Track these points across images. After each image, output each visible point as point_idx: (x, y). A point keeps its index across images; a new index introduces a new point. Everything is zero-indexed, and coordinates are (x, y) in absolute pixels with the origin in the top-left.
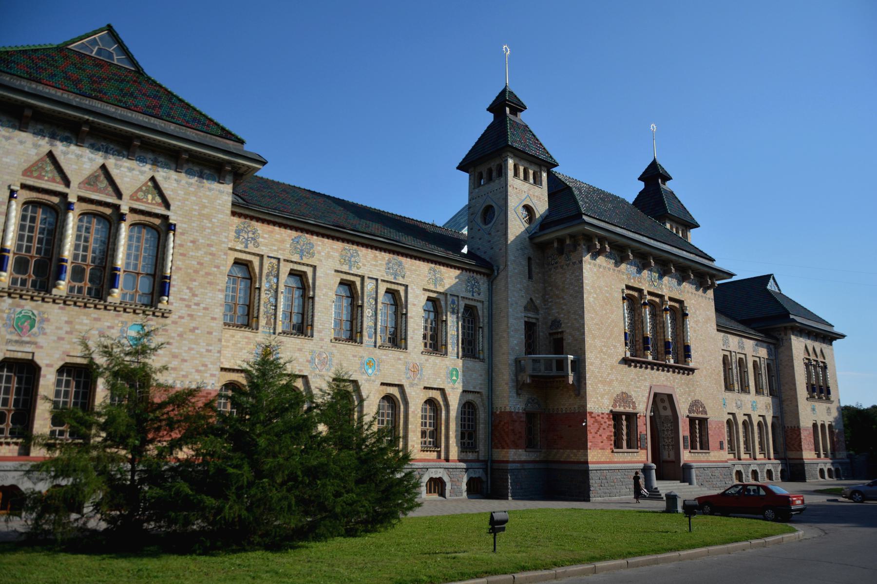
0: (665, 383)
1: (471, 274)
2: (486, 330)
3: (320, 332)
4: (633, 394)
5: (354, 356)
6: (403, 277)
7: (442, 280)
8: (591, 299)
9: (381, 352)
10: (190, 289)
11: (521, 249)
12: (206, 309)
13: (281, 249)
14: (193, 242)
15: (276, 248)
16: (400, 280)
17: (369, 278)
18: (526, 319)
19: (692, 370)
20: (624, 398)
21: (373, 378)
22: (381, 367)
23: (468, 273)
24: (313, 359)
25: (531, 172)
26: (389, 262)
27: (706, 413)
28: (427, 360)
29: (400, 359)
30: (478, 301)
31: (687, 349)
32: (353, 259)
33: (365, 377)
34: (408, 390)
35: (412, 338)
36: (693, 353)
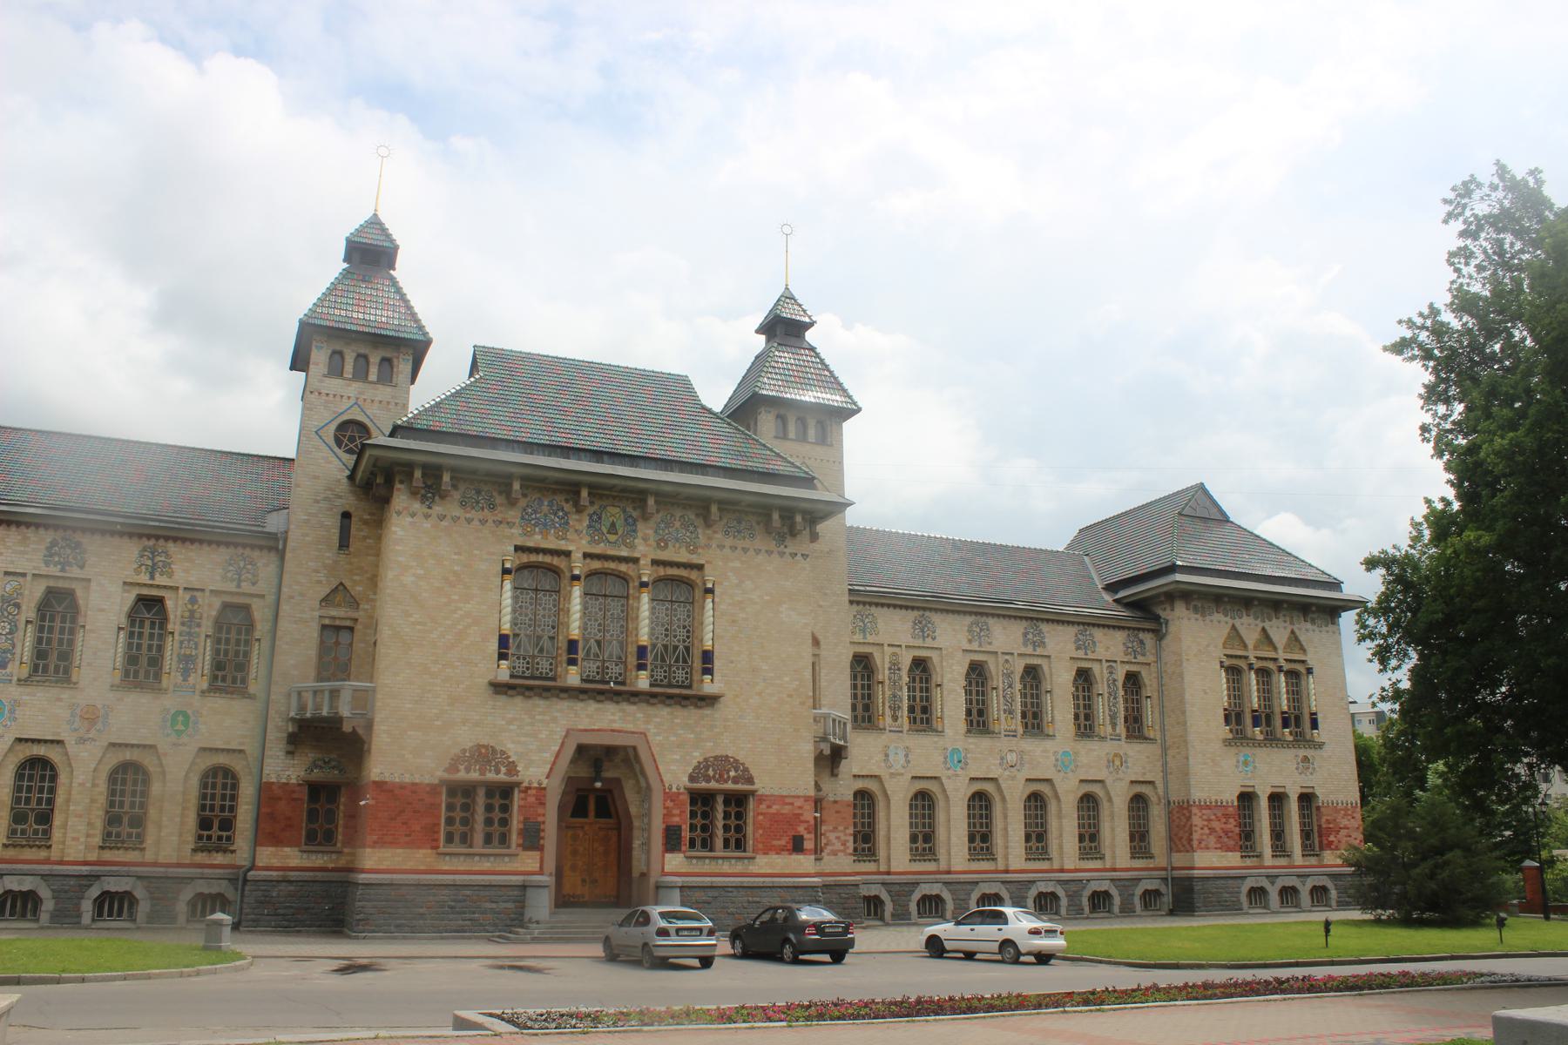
0: (616, 726)
1: (240, 550)
2: (265, 644)
4: (512, 749)
6: (82, 567)
7: (167, 565)
8: (408, 579)
9: (21, 689)
11: (326, 499)
16: (75, 572)
18: (327, 622)
19: (711, 700)
20: (486, 755)
22: (18, 713)
23: (231, 550)
25: (375, 359)
26: (54, 544)
27: (750, 780)
29: (59, 700)
30: (252, 595)
31: (707, 657)
34: (71, 747)
35: (89, 664)
36: (717, 664)
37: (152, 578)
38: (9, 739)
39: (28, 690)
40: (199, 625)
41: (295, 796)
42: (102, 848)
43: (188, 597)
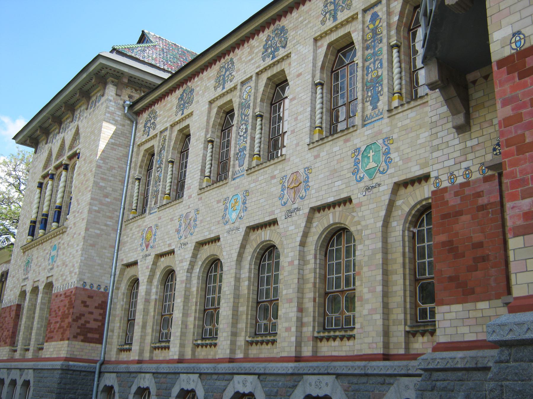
3: (189, 188)
5: (218, 202)
6: (284, 47)
10: (78, 200)
12: (81, 213)
13: (169, 117)
14: (85, 160)
15: (166, 119)
16: (282, 53)
17: (243, 83)
21: (236, 224)
24: (180, 226)
28: (316, 157)
29: (273, 177)
32: (228, 73)
33: (227, 227)
37: (335, 18)
38: (242, 231)
39: (254, 176)
40: (381, 41)
41: (482, 201)
42: (318, 339)
43: (368, 17)
